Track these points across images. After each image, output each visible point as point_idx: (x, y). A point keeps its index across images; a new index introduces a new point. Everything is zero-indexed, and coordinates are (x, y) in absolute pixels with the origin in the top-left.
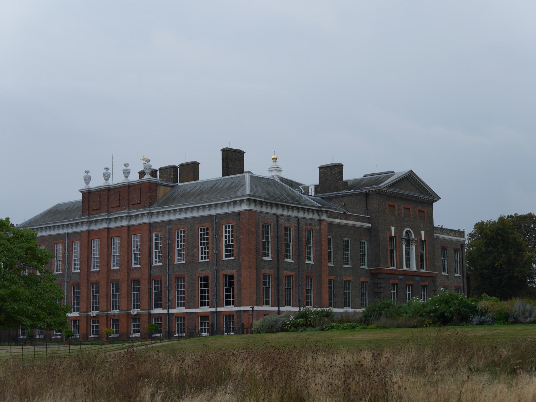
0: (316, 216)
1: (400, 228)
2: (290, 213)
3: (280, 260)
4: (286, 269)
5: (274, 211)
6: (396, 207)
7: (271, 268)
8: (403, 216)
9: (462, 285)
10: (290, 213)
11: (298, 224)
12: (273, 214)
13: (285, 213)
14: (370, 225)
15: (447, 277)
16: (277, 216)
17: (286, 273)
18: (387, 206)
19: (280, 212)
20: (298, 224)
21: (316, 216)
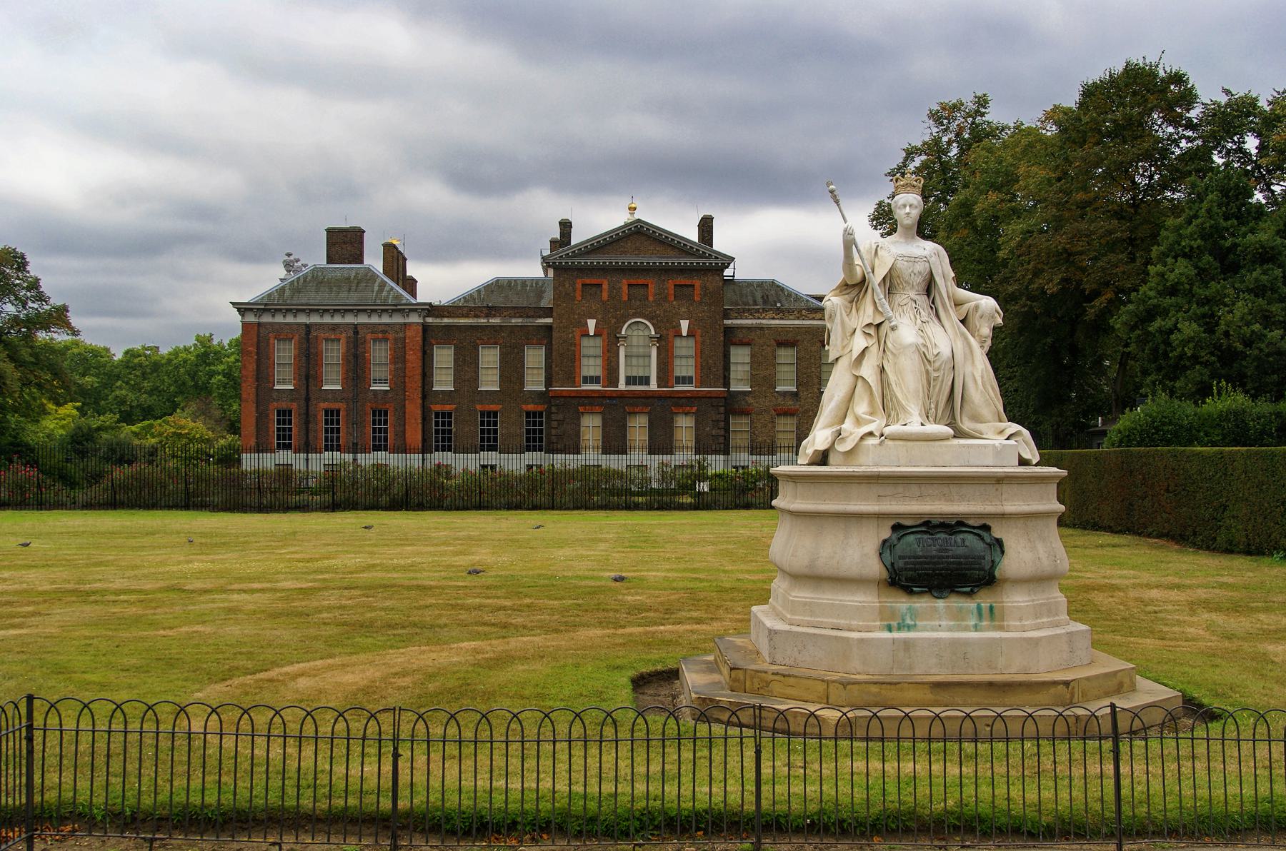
0: (398, 319)
1: (613, 321)
2: (338, 319)
5: (302, 319)
6: (605, 286)
7: (292, 400)
10: (338, 319)
11: (356, 333)
13: (327, 319)
14: (549, 320)
15: (795, 395)
16: (308, 327)
17: (323, 405)
18: (579, 286)
20: (356, 333)
21: (398, 319)
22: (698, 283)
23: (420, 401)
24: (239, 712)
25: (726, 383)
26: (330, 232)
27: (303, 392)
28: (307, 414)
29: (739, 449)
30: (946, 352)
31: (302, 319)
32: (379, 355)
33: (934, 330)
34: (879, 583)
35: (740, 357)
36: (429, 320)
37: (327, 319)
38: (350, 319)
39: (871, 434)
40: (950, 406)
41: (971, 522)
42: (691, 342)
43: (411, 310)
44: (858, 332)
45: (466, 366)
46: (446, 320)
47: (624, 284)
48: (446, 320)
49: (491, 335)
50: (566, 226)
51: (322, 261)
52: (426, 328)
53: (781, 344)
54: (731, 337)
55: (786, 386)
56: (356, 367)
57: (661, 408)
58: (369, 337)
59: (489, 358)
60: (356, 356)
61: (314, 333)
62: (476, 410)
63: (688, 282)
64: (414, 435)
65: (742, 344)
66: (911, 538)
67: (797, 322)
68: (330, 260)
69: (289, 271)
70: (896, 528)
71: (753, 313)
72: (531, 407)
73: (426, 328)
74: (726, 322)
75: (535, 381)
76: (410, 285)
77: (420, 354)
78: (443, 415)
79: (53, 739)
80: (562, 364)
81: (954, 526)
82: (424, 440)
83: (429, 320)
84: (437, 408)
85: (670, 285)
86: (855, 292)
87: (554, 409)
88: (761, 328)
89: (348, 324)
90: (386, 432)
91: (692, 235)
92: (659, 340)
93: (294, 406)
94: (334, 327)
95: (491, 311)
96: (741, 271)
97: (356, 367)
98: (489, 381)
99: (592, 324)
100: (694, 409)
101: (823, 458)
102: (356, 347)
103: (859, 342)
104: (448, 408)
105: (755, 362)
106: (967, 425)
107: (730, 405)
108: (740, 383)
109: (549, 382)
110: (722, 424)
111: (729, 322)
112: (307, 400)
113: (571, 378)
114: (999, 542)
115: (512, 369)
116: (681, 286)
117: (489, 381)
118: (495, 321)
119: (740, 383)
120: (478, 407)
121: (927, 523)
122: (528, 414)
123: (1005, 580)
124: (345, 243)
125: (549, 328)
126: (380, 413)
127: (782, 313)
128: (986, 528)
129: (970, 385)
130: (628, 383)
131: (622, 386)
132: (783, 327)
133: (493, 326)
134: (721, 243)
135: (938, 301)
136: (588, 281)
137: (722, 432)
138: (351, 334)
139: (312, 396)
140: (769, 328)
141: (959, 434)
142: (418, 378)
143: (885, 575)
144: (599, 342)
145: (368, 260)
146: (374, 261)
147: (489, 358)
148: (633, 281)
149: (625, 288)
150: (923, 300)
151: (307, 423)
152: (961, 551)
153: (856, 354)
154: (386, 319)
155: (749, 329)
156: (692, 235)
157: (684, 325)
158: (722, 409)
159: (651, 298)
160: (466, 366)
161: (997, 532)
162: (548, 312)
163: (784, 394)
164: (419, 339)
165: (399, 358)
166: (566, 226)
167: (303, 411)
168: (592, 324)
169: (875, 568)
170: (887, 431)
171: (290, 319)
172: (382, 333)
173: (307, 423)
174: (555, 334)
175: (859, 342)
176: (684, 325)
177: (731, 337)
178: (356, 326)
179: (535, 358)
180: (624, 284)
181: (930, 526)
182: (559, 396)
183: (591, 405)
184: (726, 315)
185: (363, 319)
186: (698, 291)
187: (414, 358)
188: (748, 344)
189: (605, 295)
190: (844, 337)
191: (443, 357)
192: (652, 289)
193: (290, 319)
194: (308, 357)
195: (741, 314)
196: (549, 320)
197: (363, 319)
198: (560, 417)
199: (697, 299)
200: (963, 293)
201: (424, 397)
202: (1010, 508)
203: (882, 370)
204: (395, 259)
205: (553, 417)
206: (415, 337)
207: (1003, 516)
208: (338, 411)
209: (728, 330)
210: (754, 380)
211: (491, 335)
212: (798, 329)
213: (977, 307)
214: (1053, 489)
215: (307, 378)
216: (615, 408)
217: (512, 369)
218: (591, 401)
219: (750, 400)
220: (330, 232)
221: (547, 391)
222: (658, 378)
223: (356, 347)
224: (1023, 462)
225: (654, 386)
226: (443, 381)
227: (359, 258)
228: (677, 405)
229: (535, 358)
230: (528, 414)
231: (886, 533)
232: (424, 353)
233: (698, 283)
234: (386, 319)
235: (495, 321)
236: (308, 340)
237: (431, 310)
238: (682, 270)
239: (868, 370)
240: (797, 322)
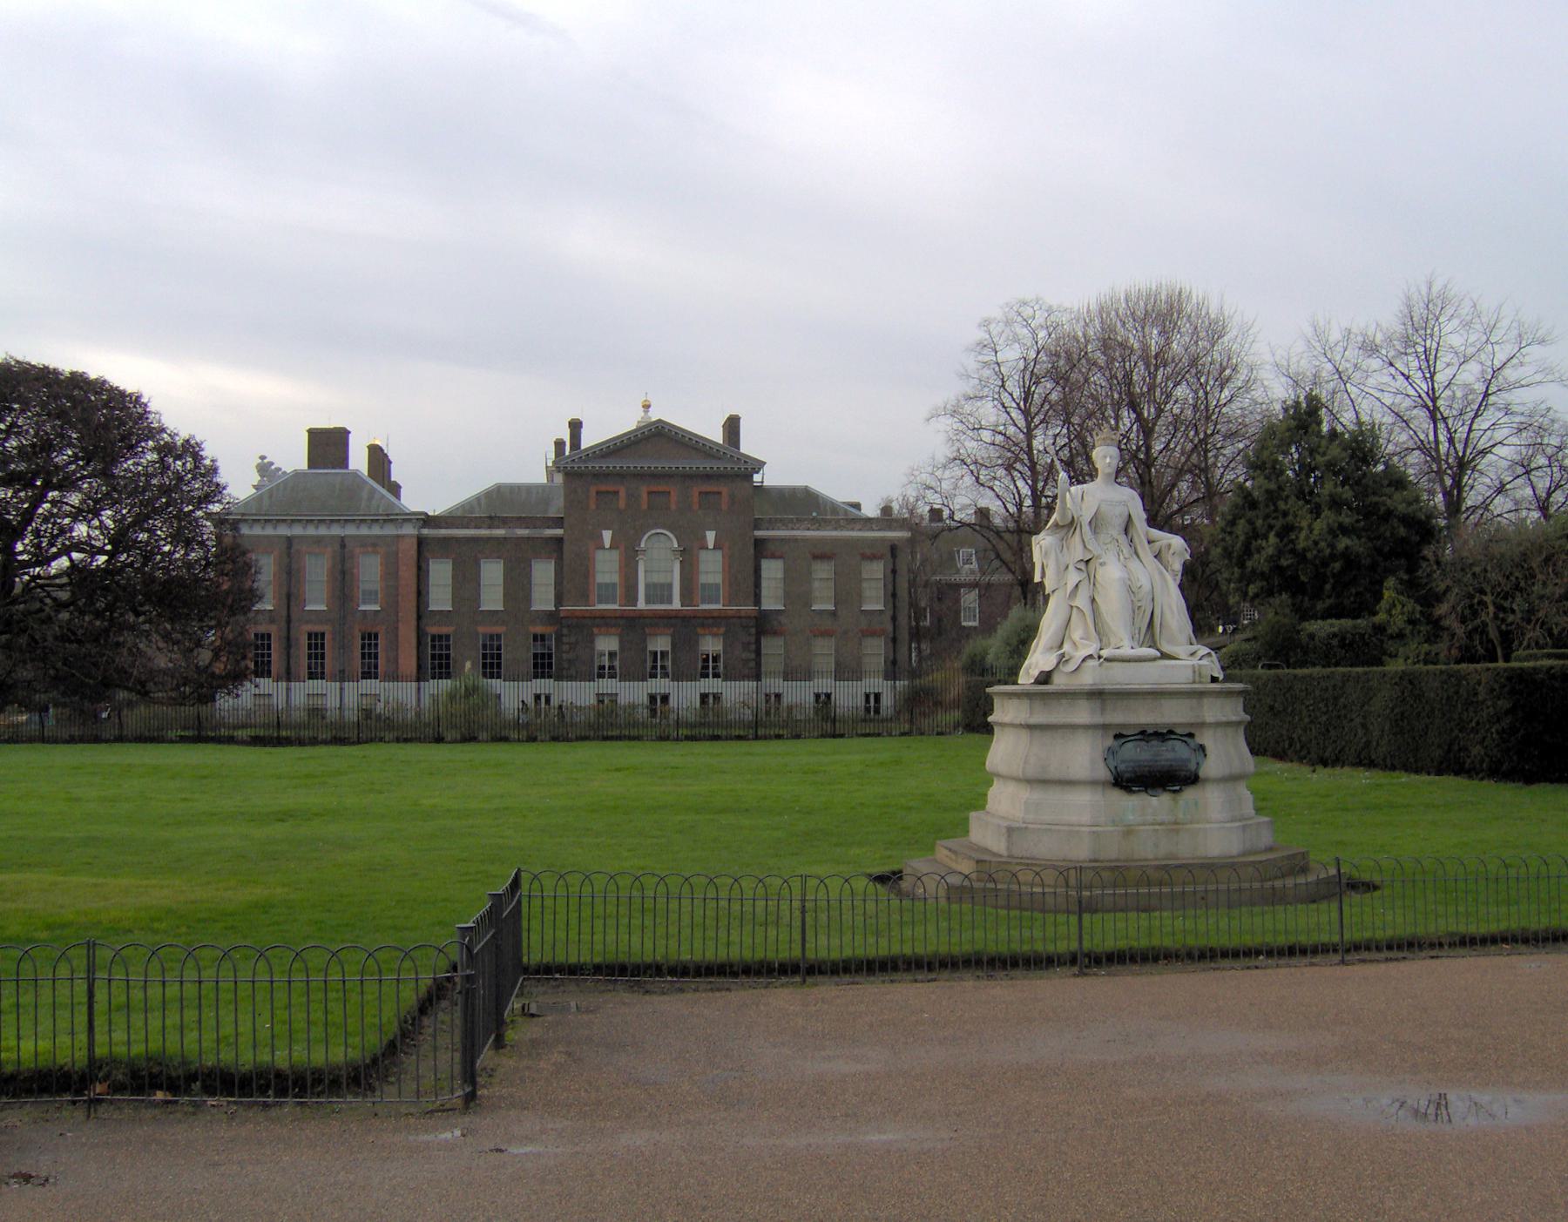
0: (390, 530)
2: (323, 531)
3: (294, 609)
4: (307, 622)
6: (622, 494)
8: (645, 507)
9: (890, 628)
10: (323, 531)
11: (343, 546)
12: (279, 537)
13: (311, 531)
14: (559, 532)
15: (833, 614)
16: (289, 541)
18: (593, 490)
19: (297, 530)
20: (343, 546)
21: (390, 530)
22: (725, 490)
23: (414, 623)
24: (681, 880)
25: (757, 600)
26: (313, 433)
27: (284, 613)
28: (288, 638)
29: (822, 674)
30: (1147, 587)
31: (283, 531)
32: (370, 571)
33: (1134, 565)
34: (1104, 784)
35: (772, 570)
36: (425, 531)
37: (311, 531)
38: (336, 531)
39: (1091, 656)
40: (1150, 632)
41: (1178, 731)
42: (719, 554)
43: (405, 520)
44: (1071, 568)
45: (466, 581)
46: (443, 532)
47: (643, 490)
48: (443, 532)
49: (495, 547)
50: (576, 426)
51: (303, 465)
52: (421, 541)
53: (816, 557)
54: (761, 549)
55: (823, 603)
56: (343, 580)
57: (685, 626)
58: (357, 550)
59: (492, 573)
60: (343, 573)
61: (295, 547)
62: (477, 634)
63: (715, 489)
64: (408, 662)
65: (773, 556)
66: (1130, 745)
67: (834, 533)
68: (310, 467)
69: (262, 476)
70: (1117, 737)
71: (785, 524)
72: (539, 629)
73: (421, 541)
74: (758, 533)
75: (543, 599)
76: (395, 489)
77: (414, 570)
78: (440, 637)
79: (536, 903)
80: (573, 579)
81: (1163, 735)
82: (419, 667)
83: (425, 531)
84: (433, 630)
85: (695, 492)
86: (1064, 532)
87: (565, 631)
88: (795, 540)
89: (333, 537)
90: (376, 658)
91: (716, 435)
92: (683, 552)
93: (273, 629)
94: (319, 540)
95: (492, 521)
96: (770, 477)
97: (343, 580)
98: (492, 597)
99: (607, 536)
100: (722, 630)
101: (1045, 678)
102: (343, 561)
103: (1073, 577)
104: (444, 630)
105: (788, 578)
106: (1166, 648)
107: (763, 624)
108: (770, 602)
109: (559, 599)
110: (753, 647)
111: (758, 533)
112: (289, 621)
113: (584, 596)
114: (1202, 748)
115: (518, 586)
116: (707, 493)
117: (492, 597)
118: (500, 532)
119: (770, 602)
120: (481, 629)
121: (1143, 733)
122: (535, 638)
123: (1206, 780)
124: (328, 445)
125: (559, 541)
126: (370, 638)
127: (820, 523)
128: (1191, 735)
129: (1168, 615)
130: (648, 601)
131: (641, 605)
132: (822, 540)
133: (497, 539)
134: (747, 447)
135: (1136, 539)
136: (603, 488)
137: (753, 656)
138: (337, 547)
139: (293, 617)
140: (805, 540)
141: (1165, 656)
142: (413, 596)
143: (1110, 778)
144: (615, 555)
145: (353, 465)
146: (358, 460)
147: (492, 573)
148: (654, 488)
149: (645, 496)
150: (1122, 539)
151: (289, 647)
152: (1170, 755)
153: (1070, 587)
154: (376, 531)
155: (783, 540)
156: (716, 435)
157: (711, 536)
158: (753, 630)
159: (673, 507)
160: (466, 581)
161: (1199, 740)
162: (558, 522)
163: (822, 612)
164: (413, 552)
165: (391, 572)
166: (576, 426)
167: (284, 633)
168: (607, 536)
169: (1103, 773)
170: (1105, 653)
171: (269, 531)
172: (372, 544)
173: (289, 647)
174: (566, 547)
175: (1073, 577)
176: (711, 536)
177: (761, 549)
178: (343, 539)
179: (543, 573)
180: (643, 490)
181: (1147, 735)
182: (572, 616)
183: (607, 625)
184: (757, 527)
185: (350, 531)
186: (725, 498)
187: (408, 574)
188: (780, 557)
189: (622, 504)
190: (1058, 573)
191: (441, 573)
192: (674, 497)
193: (269, 531)
194: (289, 573)
195: (772, 523)
196: (559, 532)
197: (350, 531)
198: (573, 639)
199: (724, 507)
200: (1155, 533)
201: (419, 618)
202: (1209, 719)
203: (1093, 600)
204: (379, 458)
205: (565, 640)
206: (409, 551)
207: (1202, 725)
208: (323, 635)
209: (759, 543)
210: (788, 596)
211: (495, 547)
212: (835, 540)
213: (1169, 546)
214: (1239, 704)
215: (289, 596)
216: (633, 625)
217: (518, 586)
218: (605, 621)
219: (783, 620)
220: (313, 433)
221: (557, 610)
222: (682, 595)
223: (343, 561)
224: (1214, 680)
225: (676, 604)
226: (440, 598)
227: (343, 461)
228: (703, 625)
229: (543, 573)
230: (535, 638)
231: (1110, 741)
232: (419, 568)
233: (725, 490)
234: (376, 531)
235: (500, 532)
236: (289, 555)
237: (427, 520)
238: (708, 477)
239: (1082, 601)
240: (834, 533)
